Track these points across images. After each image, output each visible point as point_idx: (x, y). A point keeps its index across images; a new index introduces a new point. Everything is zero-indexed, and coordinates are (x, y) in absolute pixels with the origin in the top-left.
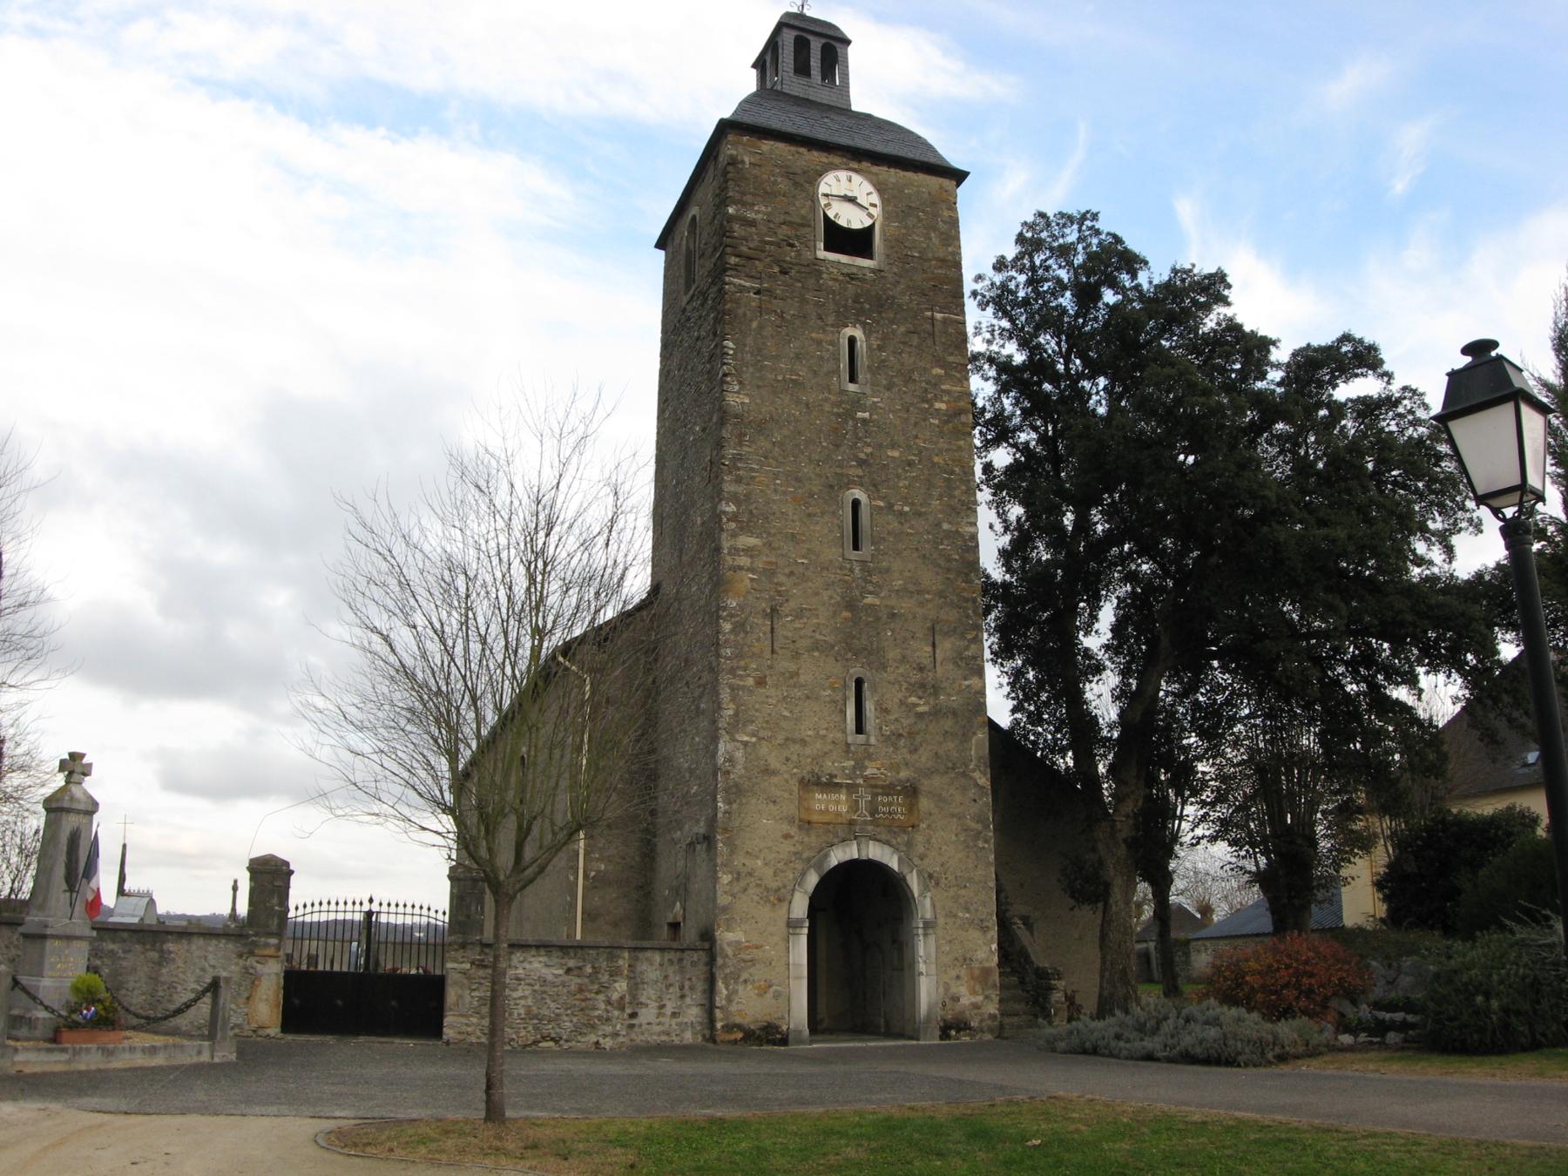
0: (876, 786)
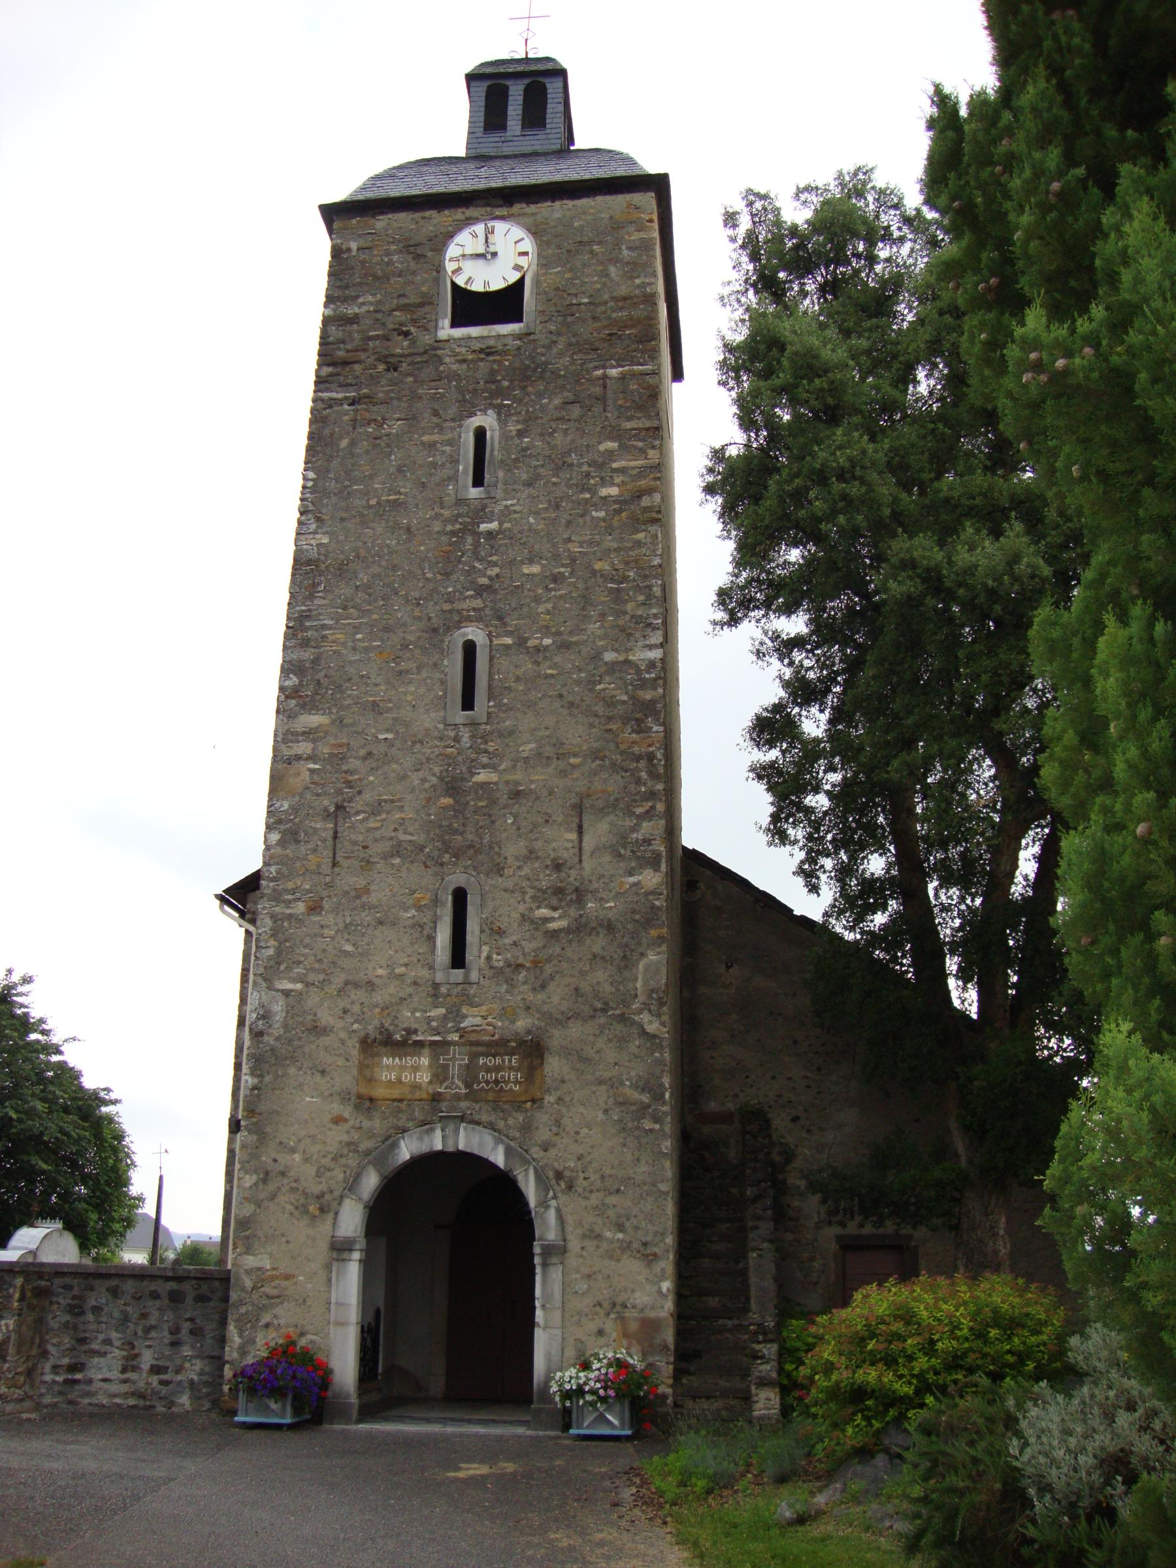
0: (478, 1043)
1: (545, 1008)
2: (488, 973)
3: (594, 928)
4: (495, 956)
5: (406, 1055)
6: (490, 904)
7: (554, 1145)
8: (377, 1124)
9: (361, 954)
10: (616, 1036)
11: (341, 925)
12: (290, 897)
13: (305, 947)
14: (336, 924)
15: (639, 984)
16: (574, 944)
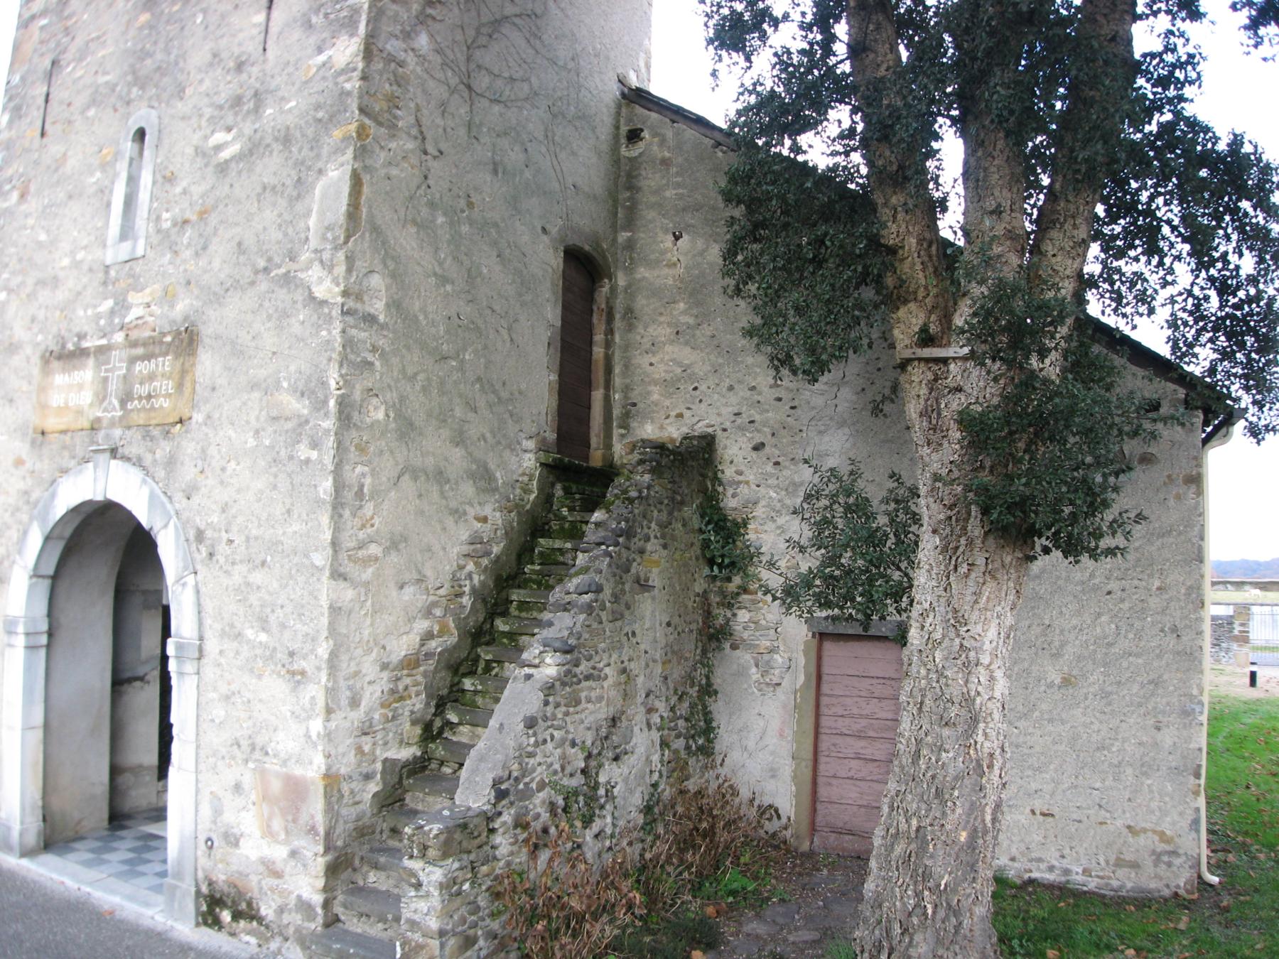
3: (268, 146)
15: (312, 222)
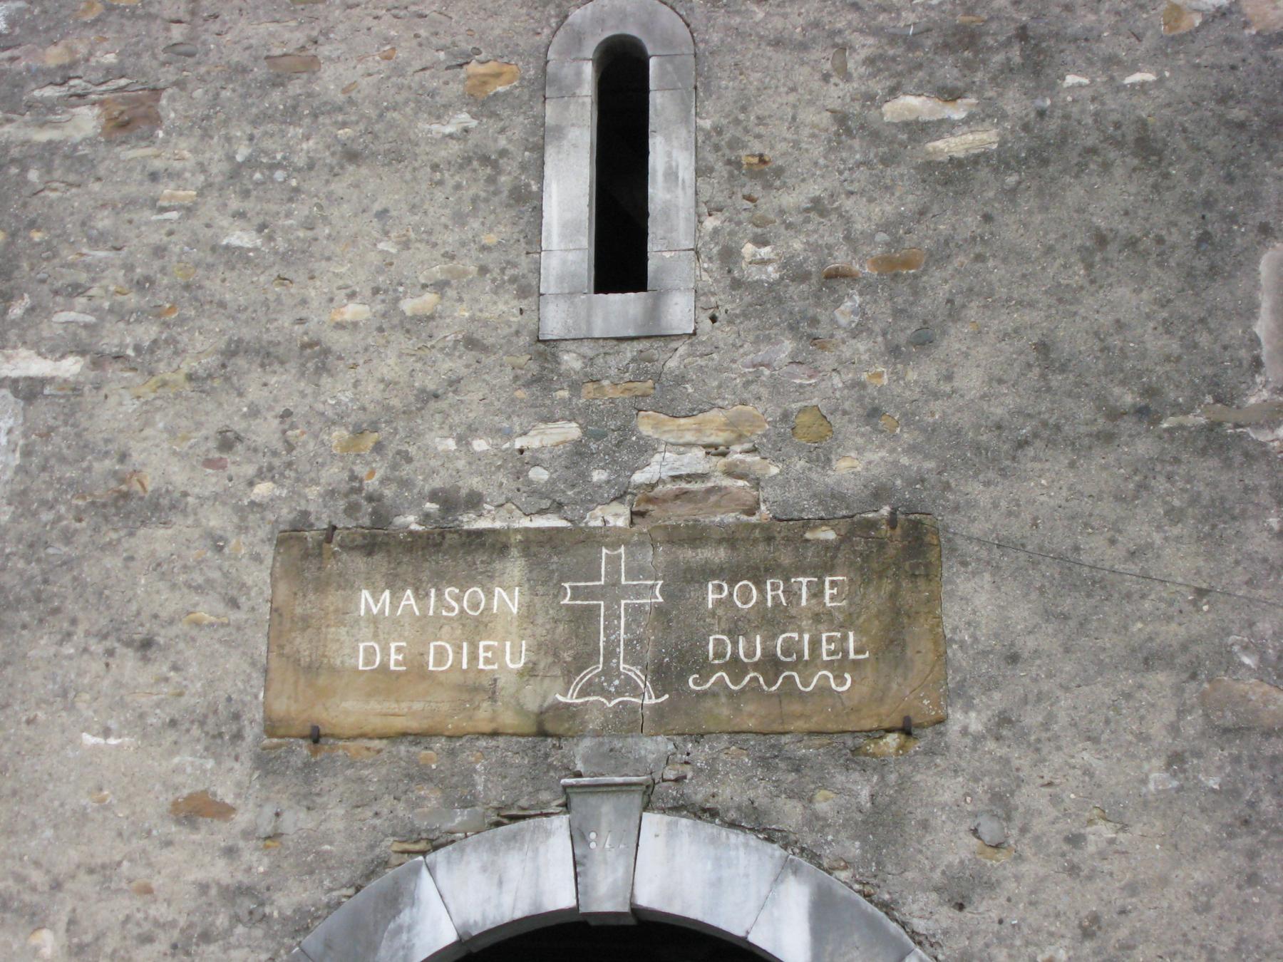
0: (696, 536)
1: (936, 411)
2: (729, 304)
3: (1093, 151)
4: (748, 249)
5: (440, 579)
6: (727, 84)
7: (991, 886)
8: (335, 821)
9: (285, 258)
10: (1195, 500)
11: (218, 169)
12: (50, 92)
13: (97, 240)
14: (202, 167)
15: (1263, 326)
16: (1027, 203)
